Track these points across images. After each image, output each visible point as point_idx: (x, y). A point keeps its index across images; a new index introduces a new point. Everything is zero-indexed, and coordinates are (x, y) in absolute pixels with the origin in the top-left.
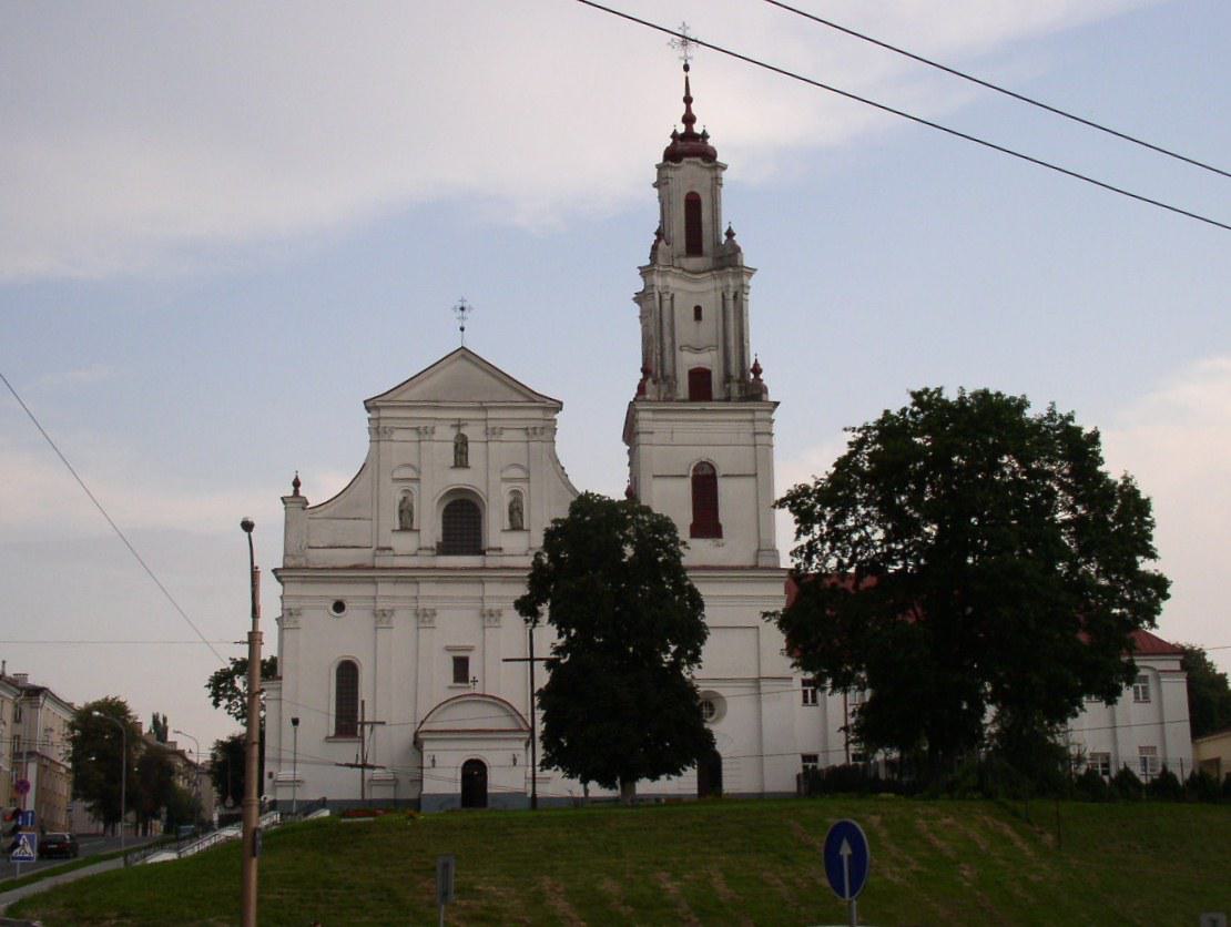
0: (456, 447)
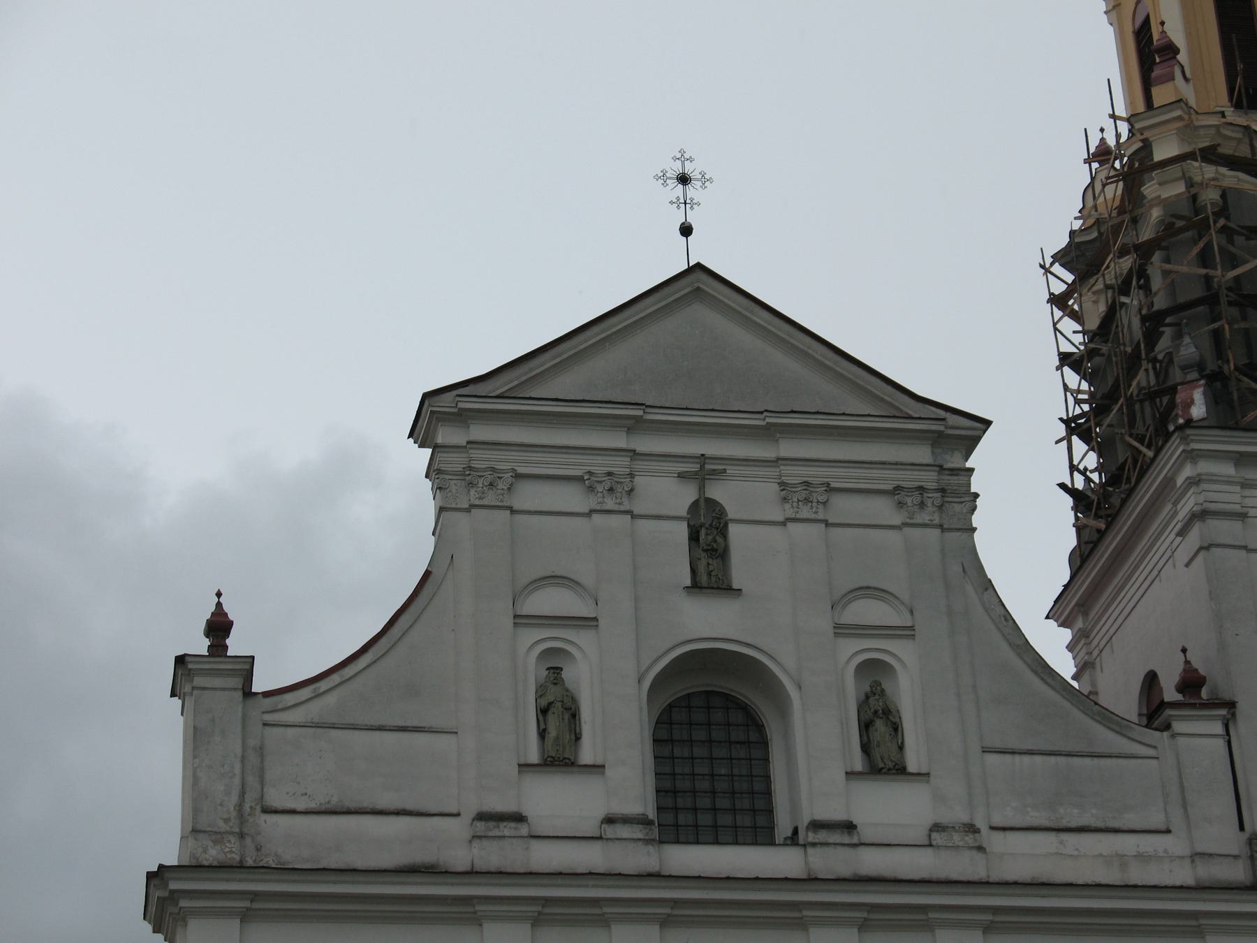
0: (694, 537)
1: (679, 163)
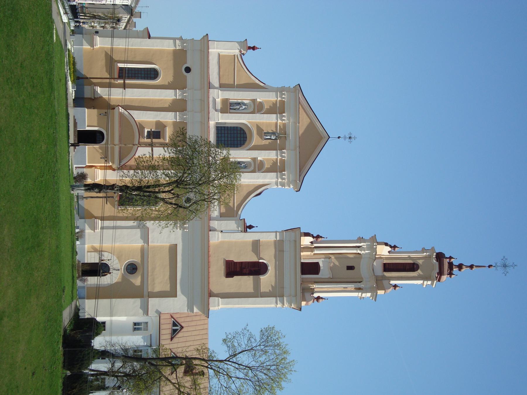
1: (354, 137)
